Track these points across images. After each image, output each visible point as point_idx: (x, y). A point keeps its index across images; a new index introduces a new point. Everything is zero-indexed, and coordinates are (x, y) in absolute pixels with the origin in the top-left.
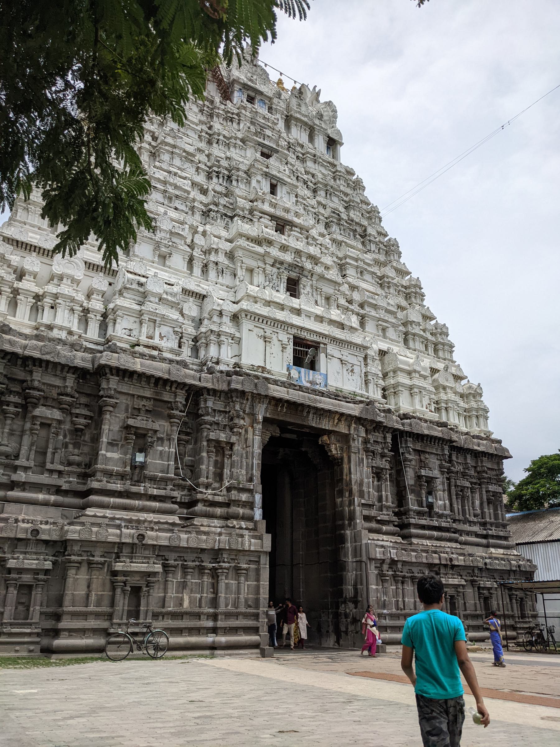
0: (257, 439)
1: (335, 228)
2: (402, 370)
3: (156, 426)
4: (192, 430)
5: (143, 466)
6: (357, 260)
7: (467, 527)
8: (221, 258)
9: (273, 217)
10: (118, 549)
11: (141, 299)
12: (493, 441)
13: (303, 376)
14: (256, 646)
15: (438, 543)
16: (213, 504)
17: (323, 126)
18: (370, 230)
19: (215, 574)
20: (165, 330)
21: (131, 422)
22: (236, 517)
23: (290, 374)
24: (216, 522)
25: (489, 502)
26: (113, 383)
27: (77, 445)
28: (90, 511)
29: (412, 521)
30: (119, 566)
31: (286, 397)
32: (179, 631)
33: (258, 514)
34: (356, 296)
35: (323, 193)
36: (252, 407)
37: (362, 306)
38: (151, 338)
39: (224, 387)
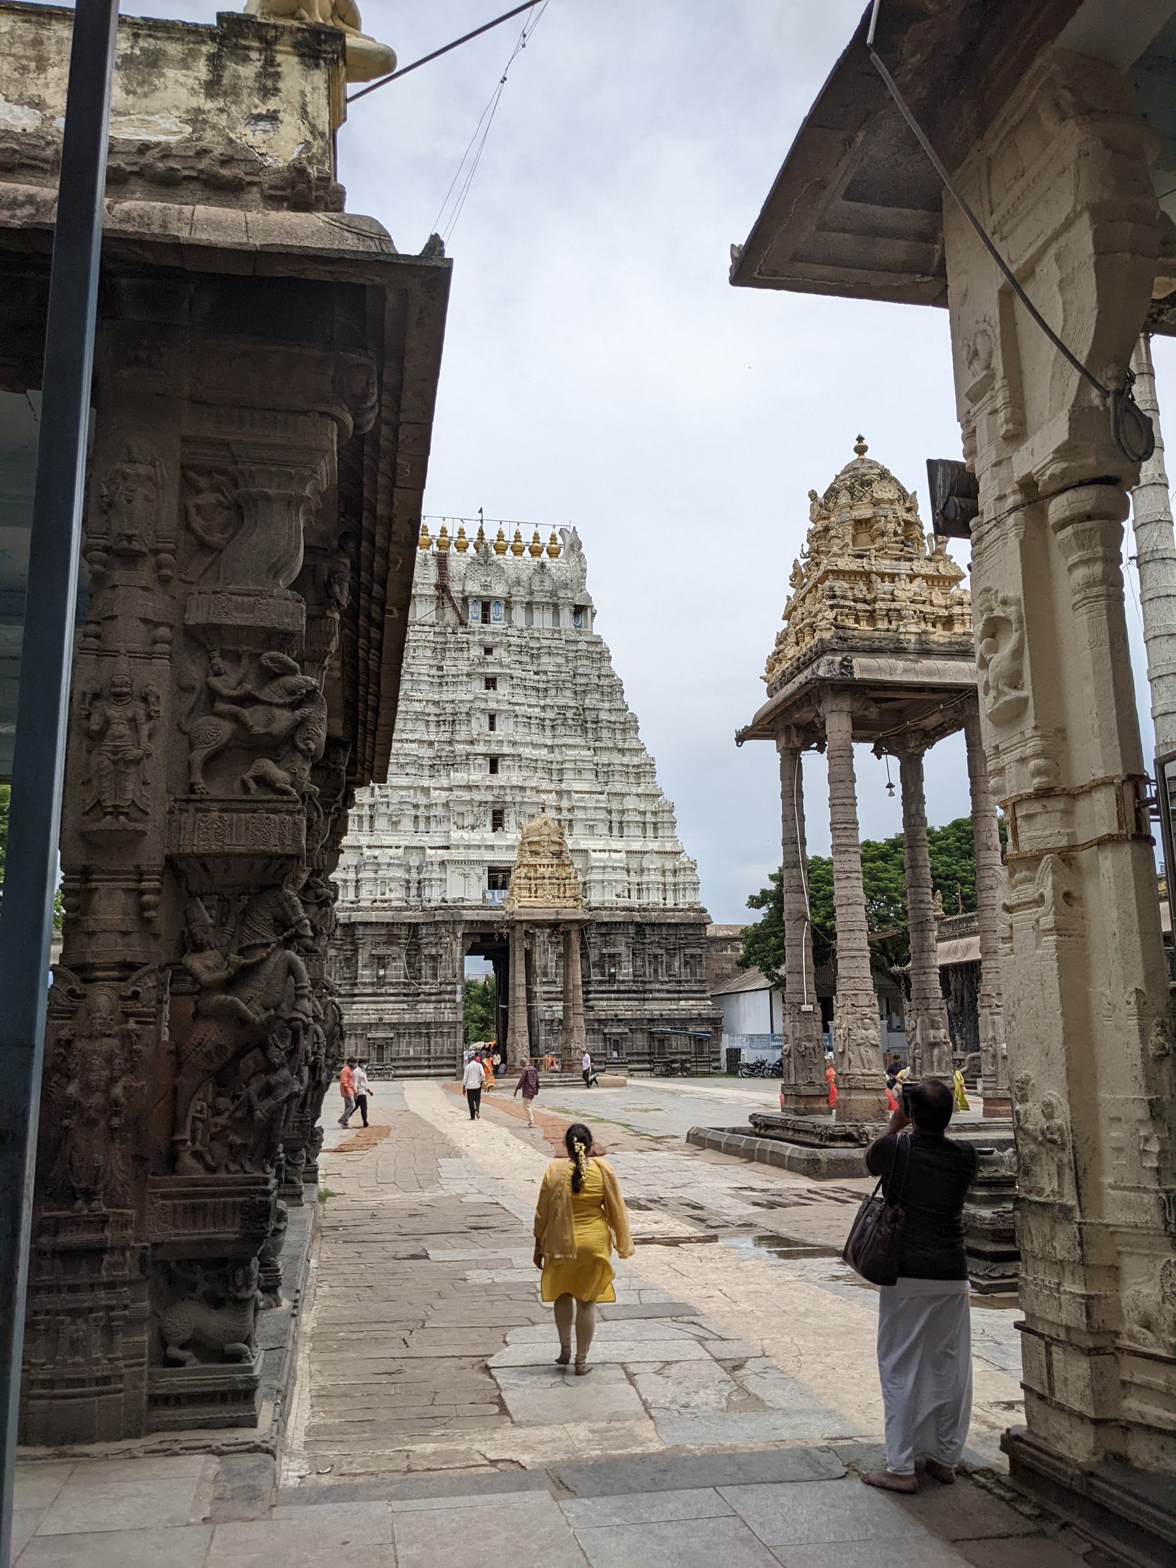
0: (459, 948)
1: (560, 730)
2: (596, 867)
3: (389, 952)
4: (414, 948)
5: (385, 976)
6: (575, 761)
7: (658, 986)
8: (439, 811)
9: (485, 755)
10: (369, 1026)
11: (374, 868)
12: (696, 910)
13: (498, 896)
14: (454, 1075)
15: (613, 1003)
16: (431, 994)
17: (570, 595)
18: (604, 716)
19: (428, 1035)
20: (393, 885)
21: (374, 952)
22: (444, 1001)
23: (484, 897)
24: (432, 1006)
25: (687, 963)
26: (360, 931)
27: (348, 967)
28: (355, 1007)
29: (591, 988)
30: (369, 1036)
31: (477, 918)
32: (408, 1067)
33: (459, 998)
34: (565, 804)
35: (553, 692)
36: (454, 928)
37: (571, 810)
38: (383, 894)
39: (432, 920)
